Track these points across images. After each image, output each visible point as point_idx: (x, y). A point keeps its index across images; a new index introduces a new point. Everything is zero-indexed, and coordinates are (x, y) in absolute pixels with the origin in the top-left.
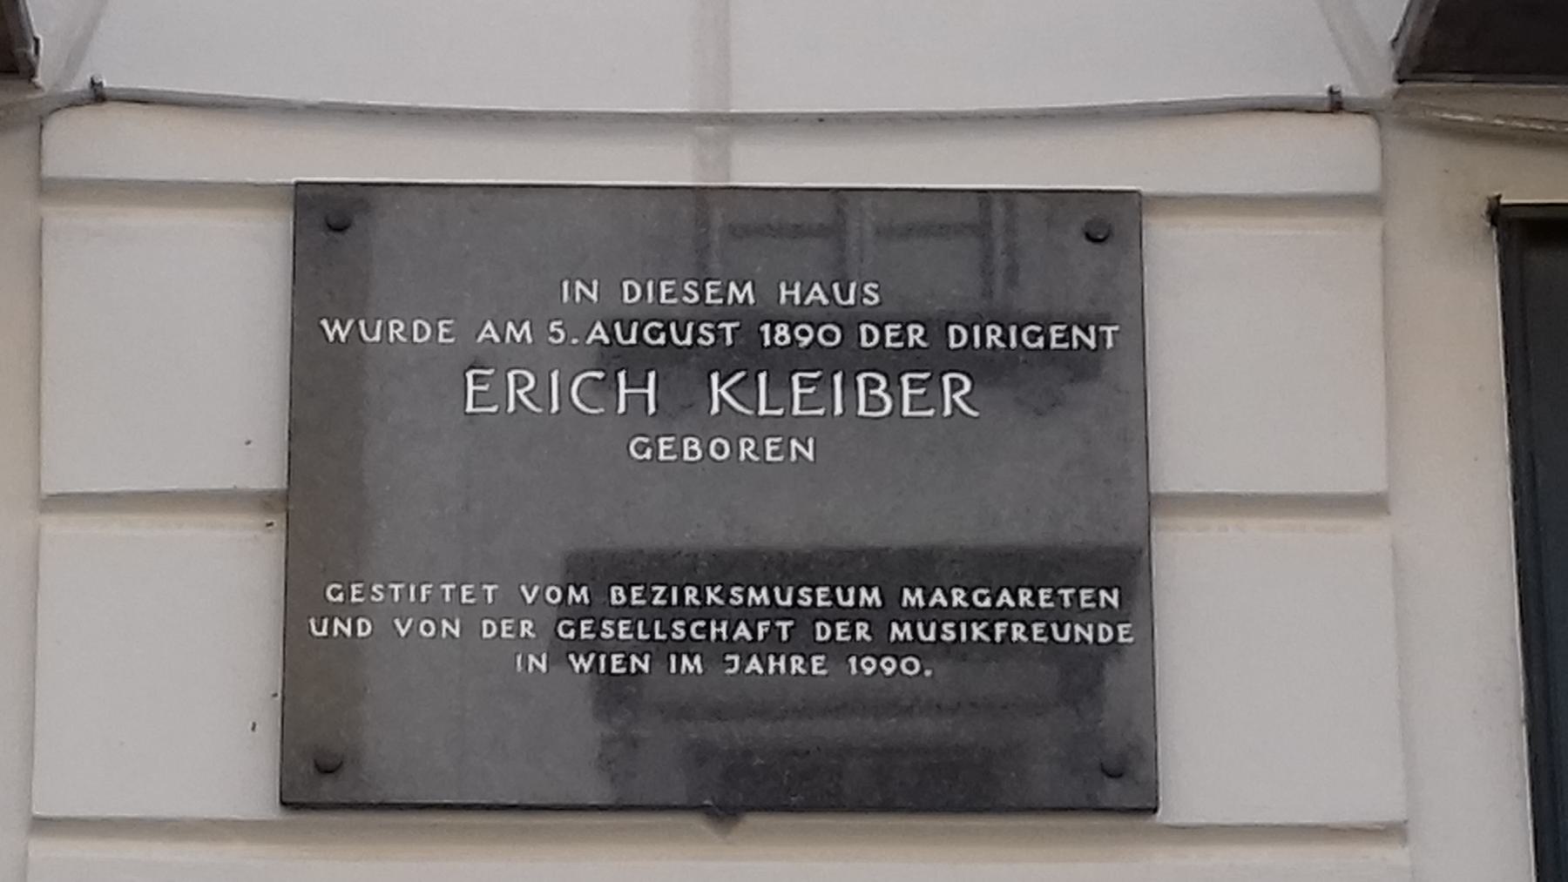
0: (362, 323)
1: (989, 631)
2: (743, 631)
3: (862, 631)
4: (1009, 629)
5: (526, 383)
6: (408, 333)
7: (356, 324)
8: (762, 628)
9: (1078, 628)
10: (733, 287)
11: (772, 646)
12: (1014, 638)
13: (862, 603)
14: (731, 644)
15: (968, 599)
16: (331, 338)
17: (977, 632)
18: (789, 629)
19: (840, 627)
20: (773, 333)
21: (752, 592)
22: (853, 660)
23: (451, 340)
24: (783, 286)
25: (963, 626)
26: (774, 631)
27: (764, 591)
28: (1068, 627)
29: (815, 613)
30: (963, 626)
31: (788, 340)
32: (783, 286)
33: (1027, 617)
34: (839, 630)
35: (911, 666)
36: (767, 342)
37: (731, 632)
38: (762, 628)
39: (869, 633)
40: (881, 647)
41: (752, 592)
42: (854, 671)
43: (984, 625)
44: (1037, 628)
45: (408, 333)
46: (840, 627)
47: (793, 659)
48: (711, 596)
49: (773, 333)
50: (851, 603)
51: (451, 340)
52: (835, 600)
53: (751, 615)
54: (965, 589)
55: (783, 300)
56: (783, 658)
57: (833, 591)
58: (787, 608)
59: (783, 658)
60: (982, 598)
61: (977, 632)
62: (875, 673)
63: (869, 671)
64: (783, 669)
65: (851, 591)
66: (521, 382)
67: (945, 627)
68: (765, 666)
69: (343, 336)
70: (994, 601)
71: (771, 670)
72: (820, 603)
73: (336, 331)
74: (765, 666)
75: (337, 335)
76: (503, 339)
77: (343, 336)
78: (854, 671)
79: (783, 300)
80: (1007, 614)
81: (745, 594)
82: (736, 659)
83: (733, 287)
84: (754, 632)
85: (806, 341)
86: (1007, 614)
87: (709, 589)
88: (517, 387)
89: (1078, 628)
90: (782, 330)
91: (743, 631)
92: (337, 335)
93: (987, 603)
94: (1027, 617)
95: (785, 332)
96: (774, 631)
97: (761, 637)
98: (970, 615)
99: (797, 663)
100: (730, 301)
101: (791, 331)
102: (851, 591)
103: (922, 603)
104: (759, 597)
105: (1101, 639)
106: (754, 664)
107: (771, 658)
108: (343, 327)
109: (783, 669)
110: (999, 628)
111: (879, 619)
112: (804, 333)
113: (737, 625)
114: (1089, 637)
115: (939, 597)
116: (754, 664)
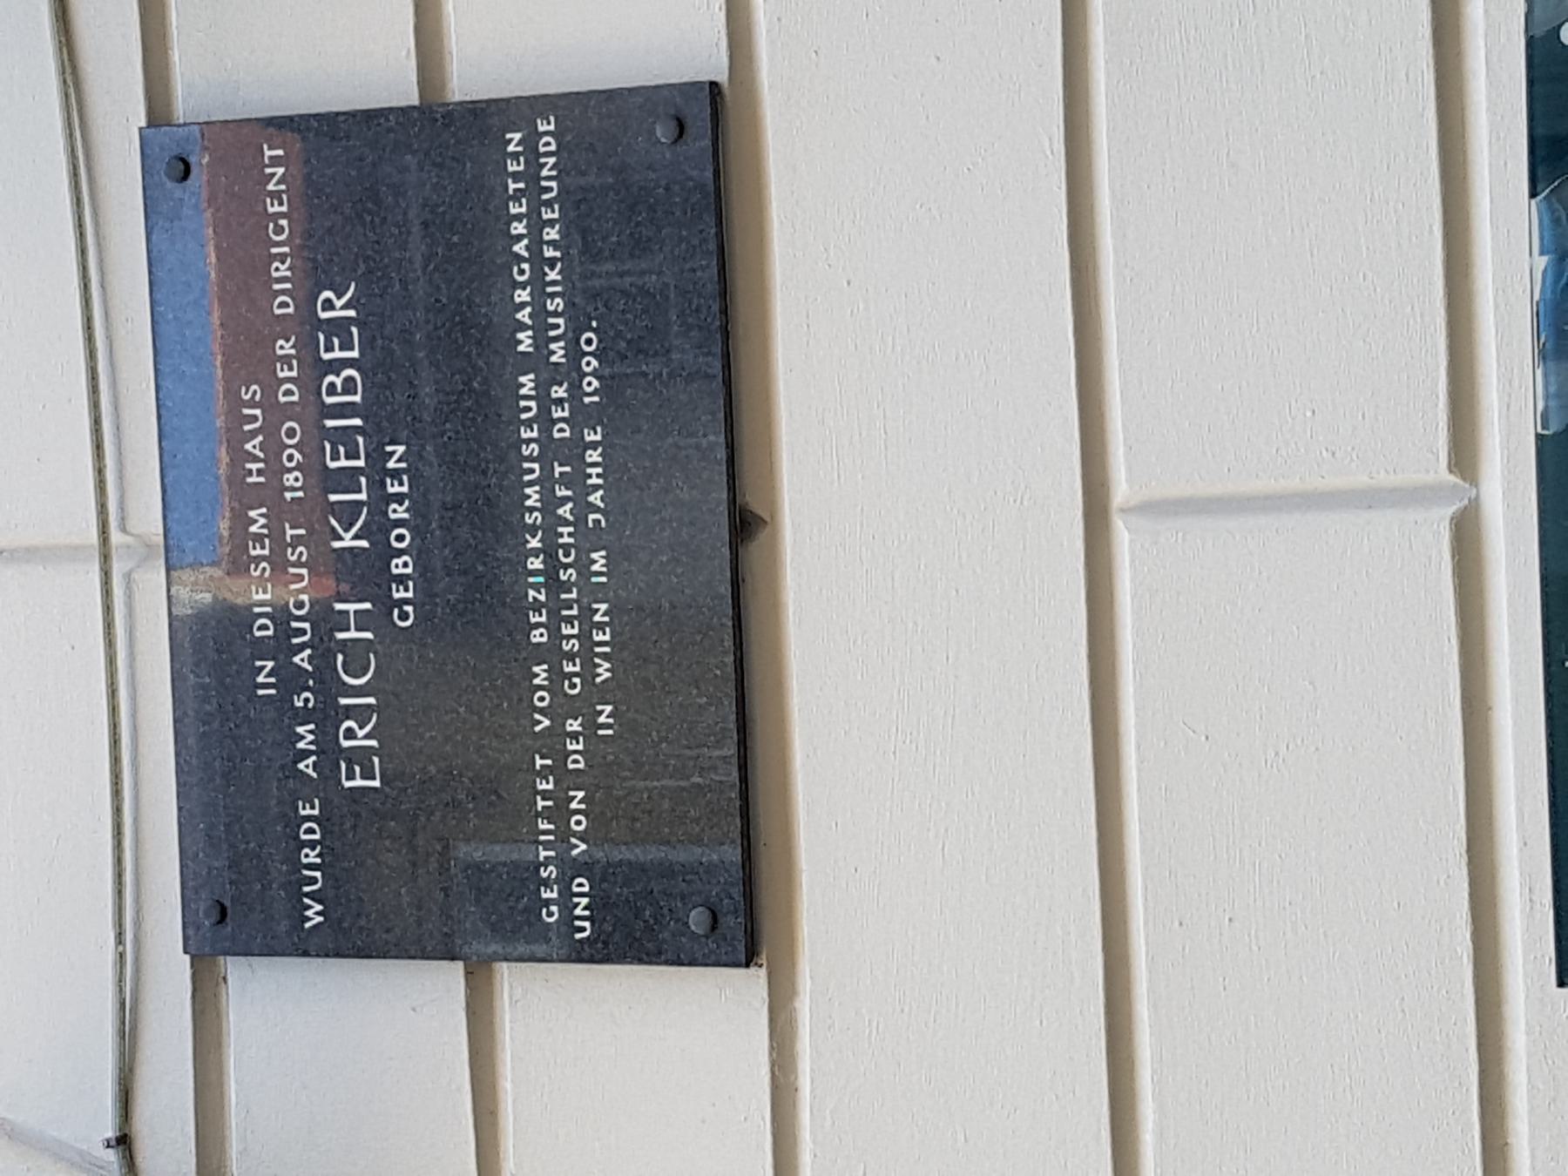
0: (307, 889)
1: (552, 263)
2: (565, 511)
3: (559, 392)
4: (549, 243)
5: (349, 730)
6: (312, 845)
7: (307, 895)
8: (562, 492)
9: (545, 173)
10: (253, 529)
11: (577, 479)
12: (557, 237)
13: (533, 393)
14: (579, 521)
15: (523, 286)
16: (321, 919)
17: (553, 275)
18: (561, 465)
19: (558, 413)
20: (294, 489)
21: (529, 503)
22: (587, 400)
23: (317, 802)
24: (250, 480)
25: (549, 289)
26: (565, 481)
27: (528, 491)
28: (544, 183)
29: (545, 440)
30: (549, 289)
31: (297, 474)
32: (250, 480)
33: (537, 226)
35: (589, 342)
36: (300, 494)
37: (567, 523)
38: (562, 492)
39: (561, 385)
40: (572, 372)
41: (529, 503)
42: (596, 399)
43: (547, 269)
44: (547, 215)
45: (312, 845)
46: (558, 413)
47: (589, 460)
48: (534, 543)
49: (294, 489)
50: (533, 404)
51: (317, 802)
52: (529, 419)
53: (550, 504)
54: (514, 289)
55: (262, 479)
56: (589, 470)
57: (523, 422)
58: (541, 469)
59: (589, 470)
60: (522, 272)
61: (553, 275)
62: (597, 378)
63: (596, 383)
64: (599, 470)
65: (523, 403)
66: (350, 734)
67: (551, 308)
68: (596, 488)
69: (319, 908)
70: (525, 260)
71: (600, 481)
72: (535, 434)
73: (314, 914)
74: (596, 488)
75: (317, 913)
76: (311, 753)
77: (319, 908)
78: (596, 399)
79: (262, 479)
80: (537, 243)
81: (532, 510)
82: (591, 517)
83: (253, 529)
84: (565, 500)
85: (297, 456)
86: (537, 243)
87: (529, 546)
88: (355, 737)
89: (545, 173)
90: (289, 479)
91: (565, 511)
92: (317, 913)
94: (537, 226)
95: (291, 476)
96: (565, 481)
97: (569, 493)
98: (538, 283)
99: (593, 456)
100: (265, 531)
101: (290, 470)
102: (523, 403)
103: (530, 333)
104: (533, 497)
105: (553, 148)
106: (595, 498)
107: (590, 482)
108: (310, 907)
109: (599, 470)
110: (549, 253)
111: (549, 375)
112: (290, 458)
113: (560, 517)
114: (552, 160)
115: (524, 316)
116: (595, 498)
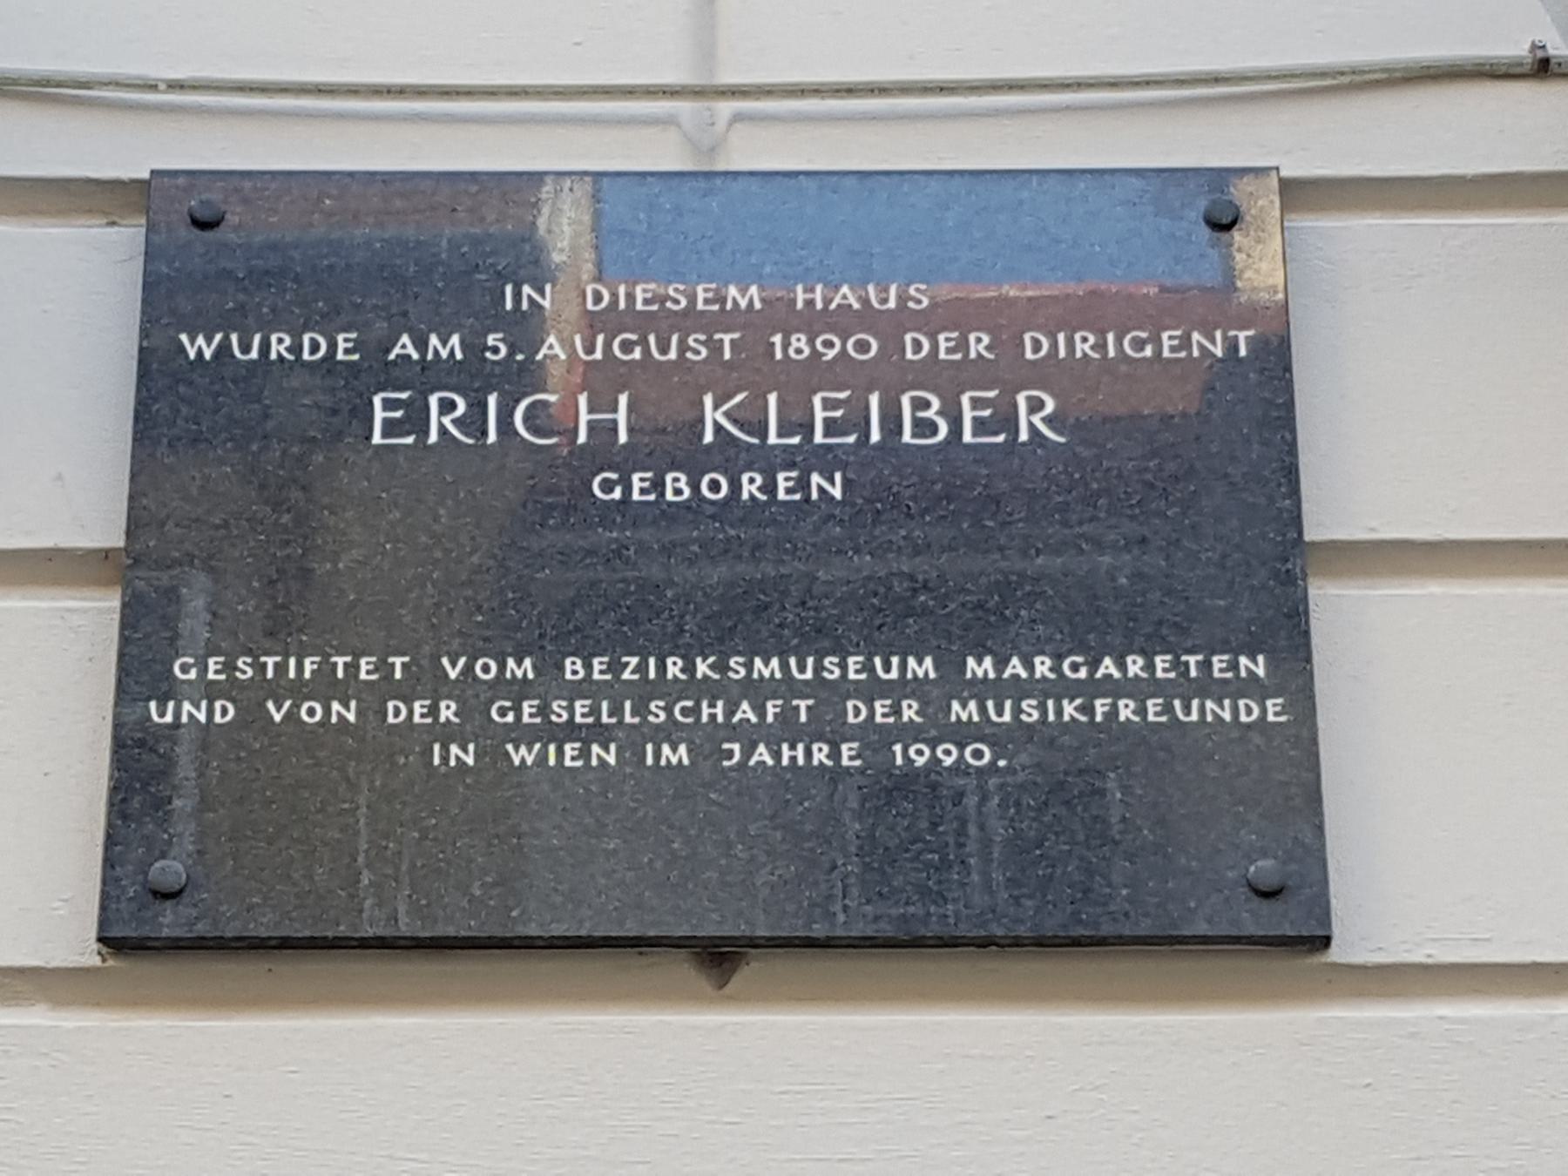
0: (234, 338)
1: (1088, 709)
2: (746, 711)
3: (910, 712)
4: (1114, 706)
6: (296, 349)
7: (227, 338)
8: (771, 709)
9: (1209, 705)
11: (788, 730)
12: (1122, 718)
13: (909, 675)
15: (1056, 669)
17: (1069, 709)
20: (786, 345)
21: (758, 662)
22: (898, 748)
23: (356, 357)
25: (1050, 703)
27: (775, 662)
28: (1195, 703)
30: (1050, 703)
31: (807, 351)
33: (1139, 690)
34: (879, 710)
36: (779, 355)
37: (729, 713)
38: (771, 709)
40: (938, 730)
41: (758, 662)
42: (899, 761)
43: (1078, 701)
44: (1153, 705)
47: (815, 747)
48: (702, 668)
49: (786, 345)
50: (894, 674)
51: (356, 357)
52: (872, 670)
53: (756, 691)
54: (1051, 656)
56: (800, 747)
57: (870, 659)
58: (806, 682)
59: (800, 747)
60: (1075, 667)
61: (1069, 709)
63: (920, 761)
64: (801, 761)
65: (895, 660)
68: (777, 755)
69: (208, 354)
70: (1091, 673)
71: (785, 762)
72: (852, 676)
73: (200, 346)
74: (777, 755)
75: (200, 353)
76: (423, 353)
77: (208, 354)
78: (899, 761)
80: (1114, 689)
81: (749, 666)
82: (736, 747)
84: (762, 714)
85: (831, 354)
86: (1114, 689)
87: (699, 660)
88: (441, 413)
89: (1209, 705)
90: (799, 341)
91: (746, 711)
92: (200, 353)
93: (1083, 673)
94: (1139, 690)
95: (803, 345)
97: (770, 719)
98: (1060, 689)
100: (729, 306)
101: (811, 342)
102: (895, 660)
103: (992, 675)
105: (1243, 718)
106: (762, 754)
107: (785, 747)
109: (801, 761)
110: (1101, 706)
112: (829, 344)
113: (737, 705)
114: (1227, 716)
115: (1015, 667)
116: (762, 754)
